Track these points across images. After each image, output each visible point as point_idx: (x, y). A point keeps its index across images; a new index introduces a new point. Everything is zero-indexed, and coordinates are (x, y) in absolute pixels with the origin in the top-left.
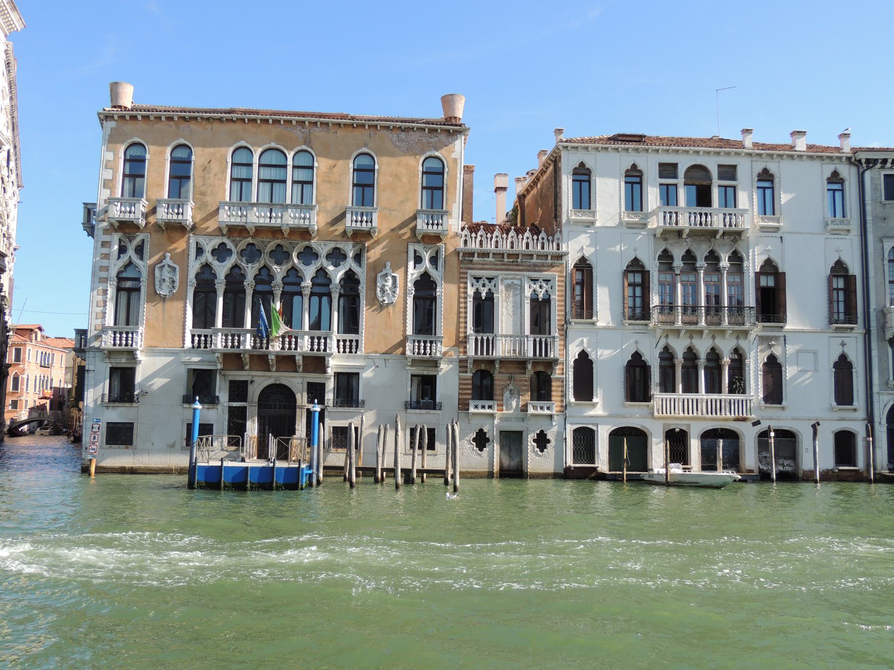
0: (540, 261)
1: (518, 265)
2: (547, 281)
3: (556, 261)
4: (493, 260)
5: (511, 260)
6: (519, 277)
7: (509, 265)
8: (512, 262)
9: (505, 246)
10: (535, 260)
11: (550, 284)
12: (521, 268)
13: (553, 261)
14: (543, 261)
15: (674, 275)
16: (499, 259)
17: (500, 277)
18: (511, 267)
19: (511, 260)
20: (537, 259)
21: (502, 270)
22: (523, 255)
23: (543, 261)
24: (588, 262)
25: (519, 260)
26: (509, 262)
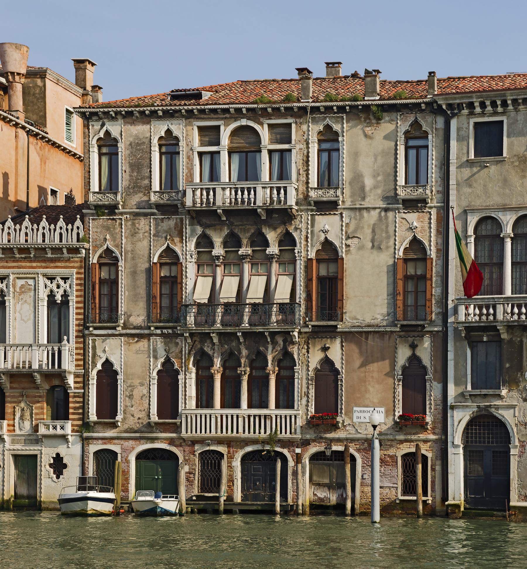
0: (53, 256)
1: (31, 261)
2: (65, 279)
3: (74, 256)
4: (3, 256)
5: (23, 256)
6: (33, 276)
7: (21, 261)
8: (25, 258)
9: (17, 239)
10: (49, 255)
11: (68, 282)
12: (34, 264)
13: (71, 256)
14: (59, 256)
15: (214, 265)
16: (10, 255)
17: (12, 277)
18: (23, 264)
19: (23, 256)
20: (68, 253)
21: (13, 267)
22: (35, 249)
23: (59, 256)
24: (114, 255)
25: (32, 256)
26: (21, 257)
